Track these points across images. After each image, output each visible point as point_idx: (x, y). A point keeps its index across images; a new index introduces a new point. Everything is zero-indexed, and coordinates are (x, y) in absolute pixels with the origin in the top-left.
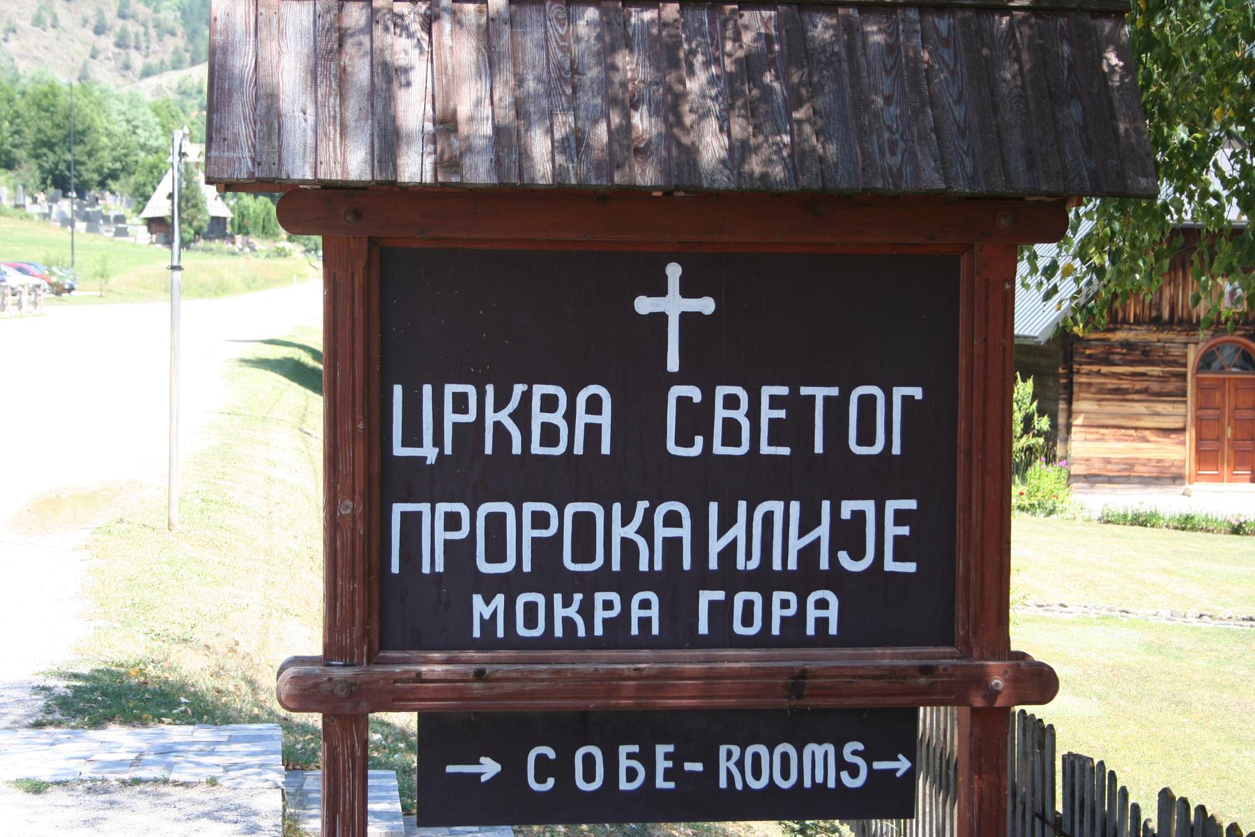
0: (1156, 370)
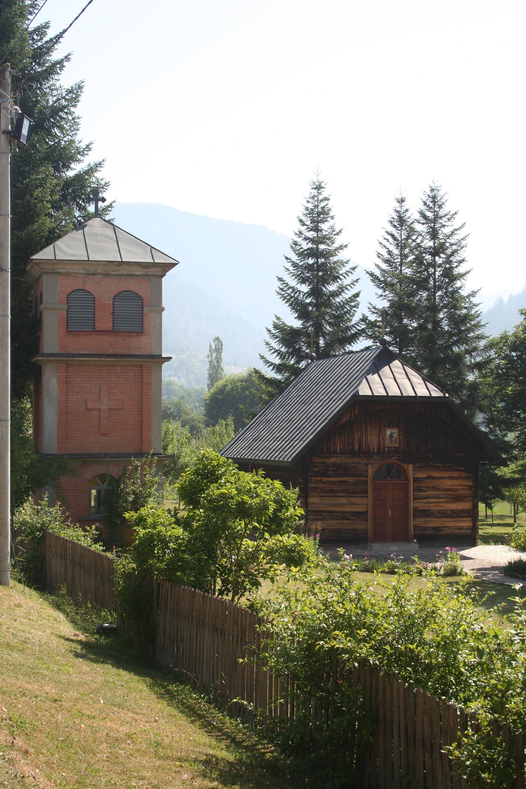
0: (351, 479)
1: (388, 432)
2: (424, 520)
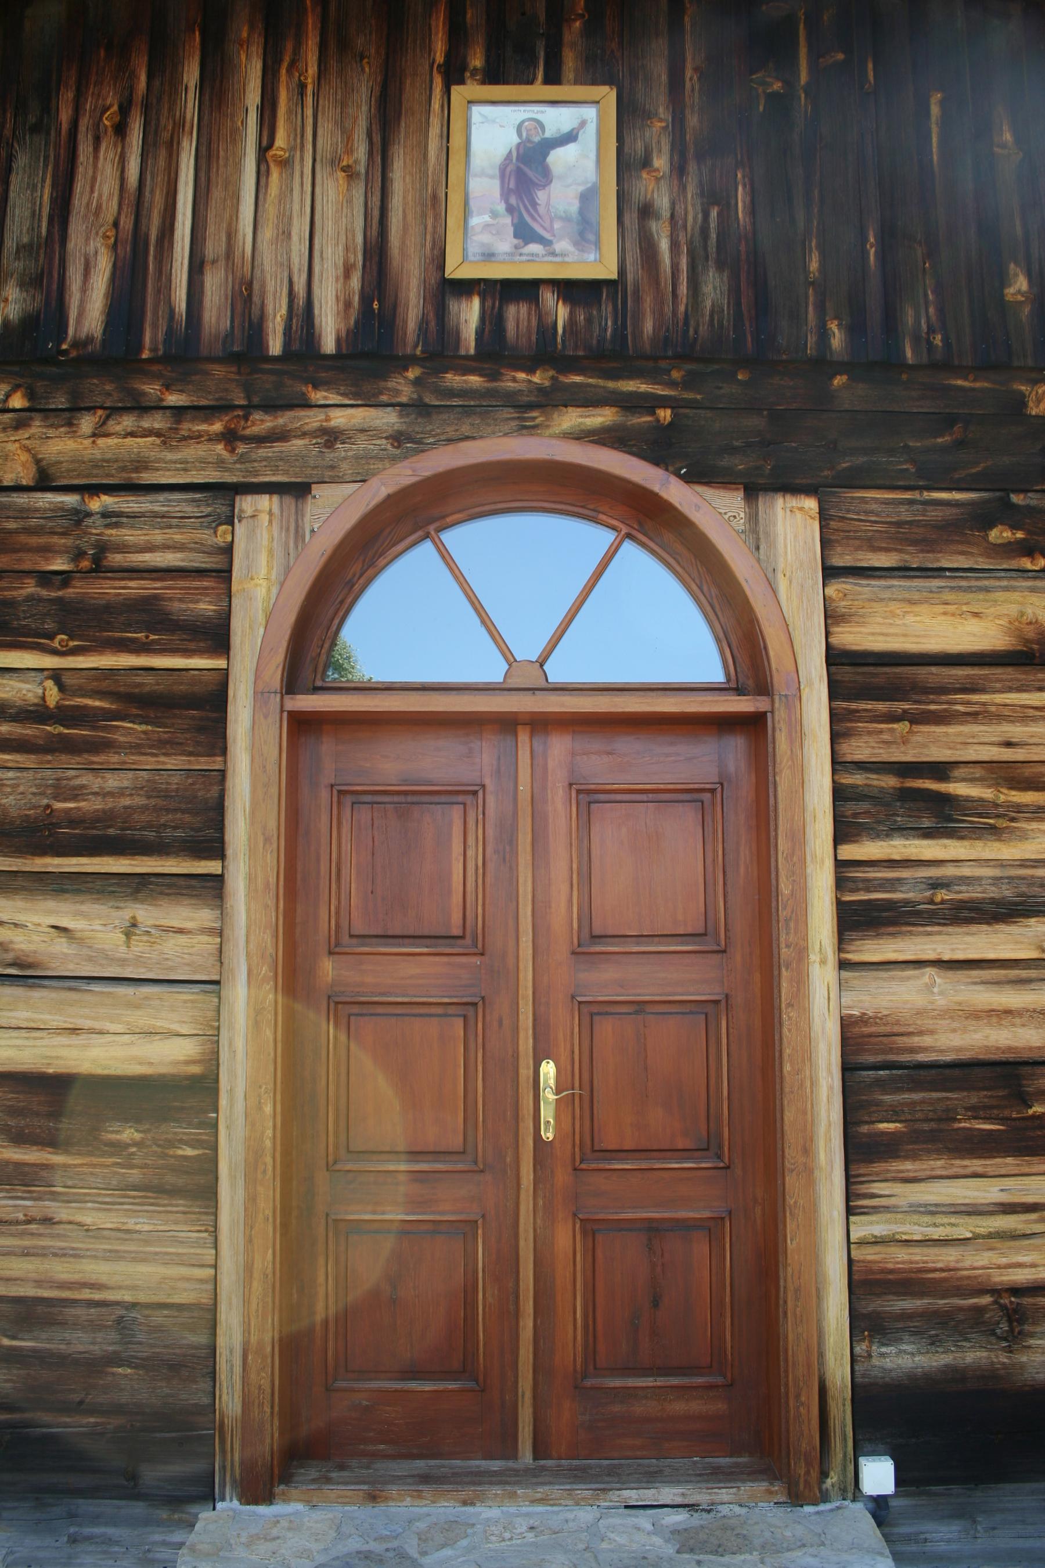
1: (492, 127)
2: (990, 1192)
